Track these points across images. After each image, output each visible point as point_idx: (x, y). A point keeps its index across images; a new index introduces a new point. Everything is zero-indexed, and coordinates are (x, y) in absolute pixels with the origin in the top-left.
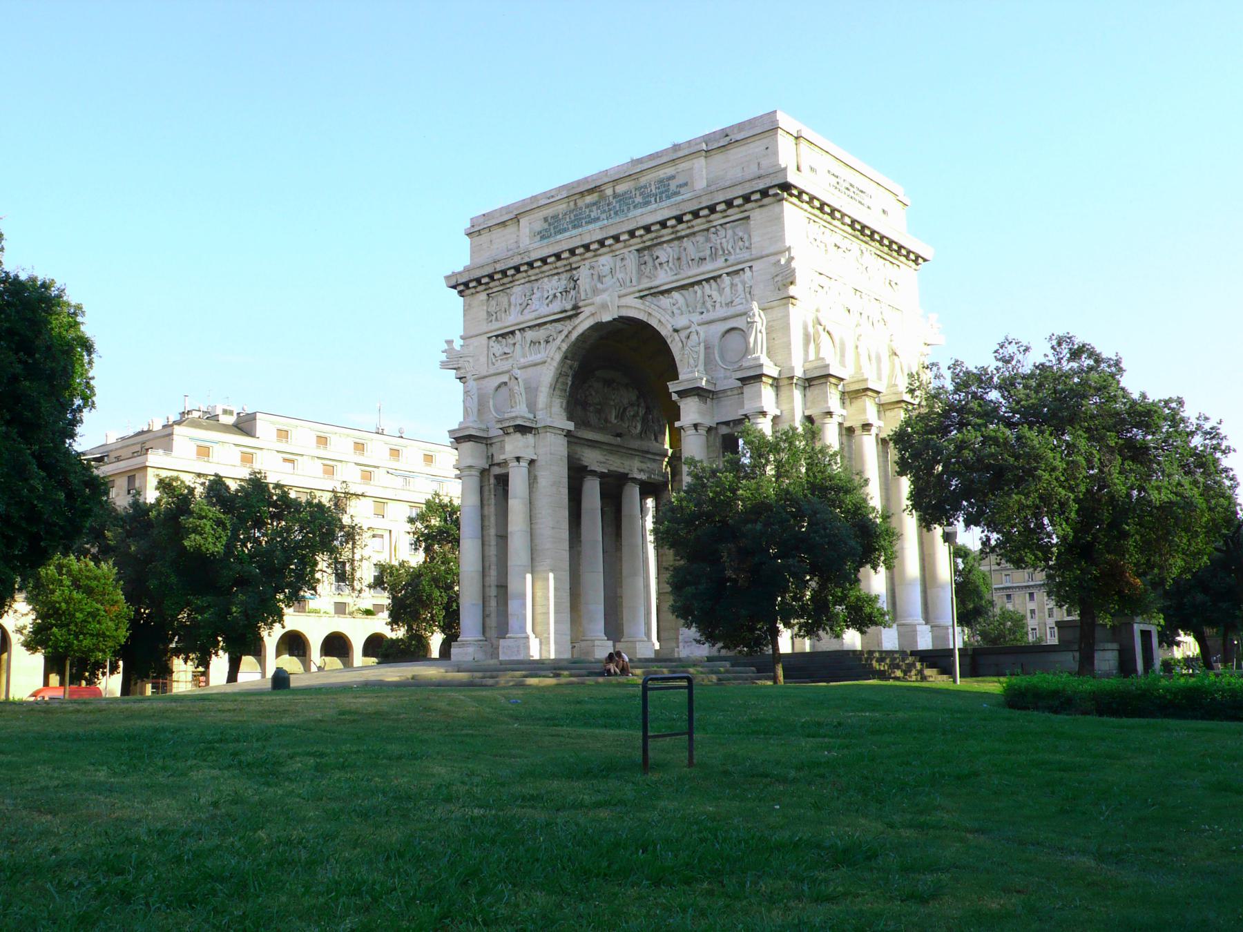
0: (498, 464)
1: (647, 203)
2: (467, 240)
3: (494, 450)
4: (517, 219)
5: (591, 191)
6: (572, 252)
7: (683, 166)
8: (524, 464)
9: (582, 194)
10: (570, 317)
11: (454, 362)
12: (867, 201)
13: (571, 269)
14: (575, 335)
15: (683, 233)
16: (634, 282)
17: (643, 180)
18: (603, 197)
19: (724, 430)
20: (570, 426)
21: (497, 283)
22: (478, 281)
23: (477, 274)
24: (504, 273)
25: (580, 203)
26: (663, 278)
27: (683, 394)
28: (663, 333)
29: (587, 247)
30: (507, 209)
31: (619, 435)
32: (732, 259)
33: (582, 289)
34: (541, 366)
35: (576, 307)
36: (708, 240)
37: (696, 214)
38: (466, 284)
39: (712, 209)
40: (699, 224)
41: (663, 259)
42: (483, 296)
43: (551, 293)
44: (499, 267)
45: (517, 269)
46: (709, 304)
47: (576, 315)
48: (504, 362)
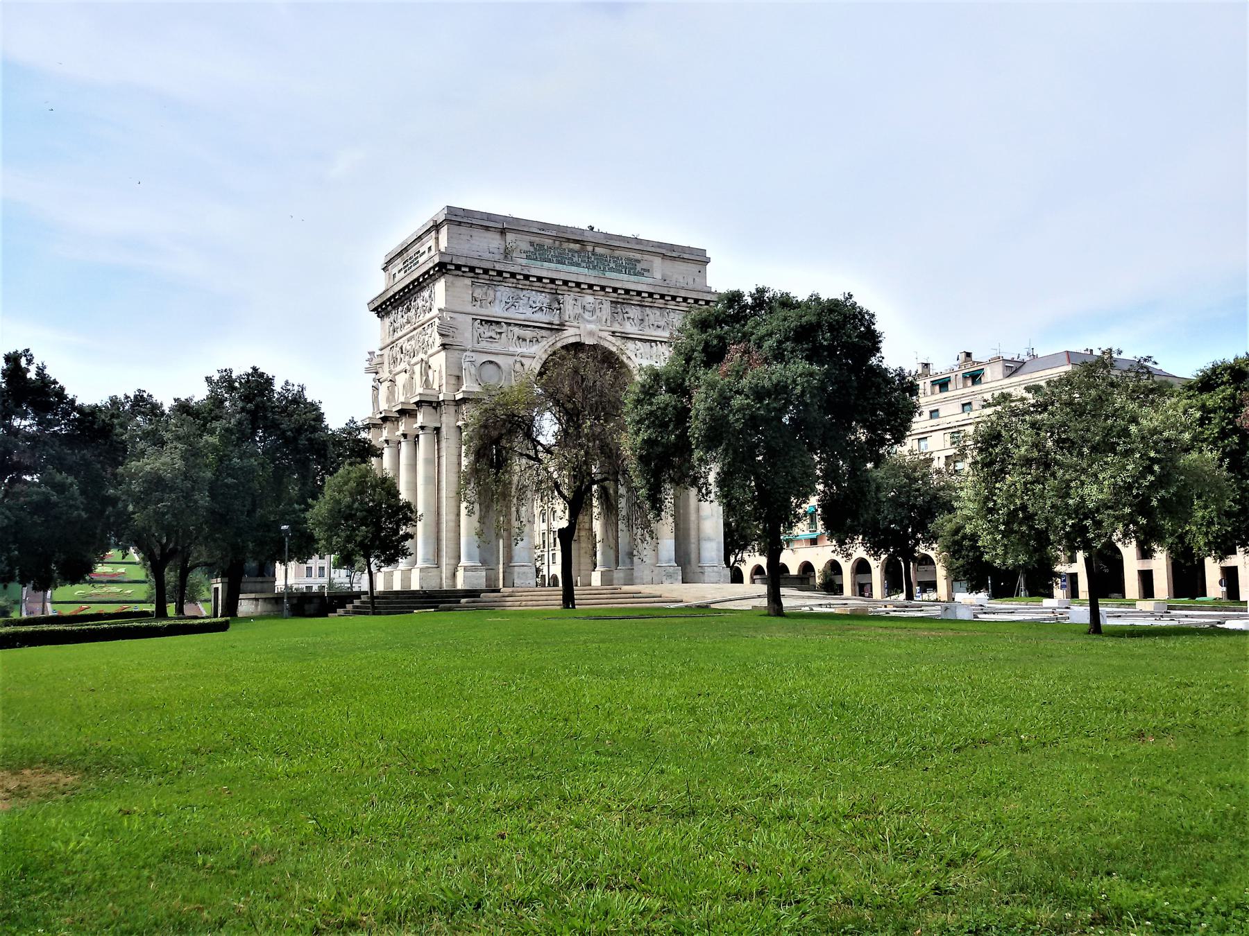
6: (566, 283)
7: (646, 257)
9: (569, 240)
10: (551, 329)
17: (617, 253)
18: (583, 249)
22: (472, 269)
23: (474, 263)
24: (500, 273)
25: (565, 245)
26: (630, 328)
29: (578, 284)
30: (489, 217)
35: (562, 324)
37: (662, 296)
38: (458, 267)
39: (674, 298)
43: (539, 305)
44: (499, 267)
45: (513, 275)
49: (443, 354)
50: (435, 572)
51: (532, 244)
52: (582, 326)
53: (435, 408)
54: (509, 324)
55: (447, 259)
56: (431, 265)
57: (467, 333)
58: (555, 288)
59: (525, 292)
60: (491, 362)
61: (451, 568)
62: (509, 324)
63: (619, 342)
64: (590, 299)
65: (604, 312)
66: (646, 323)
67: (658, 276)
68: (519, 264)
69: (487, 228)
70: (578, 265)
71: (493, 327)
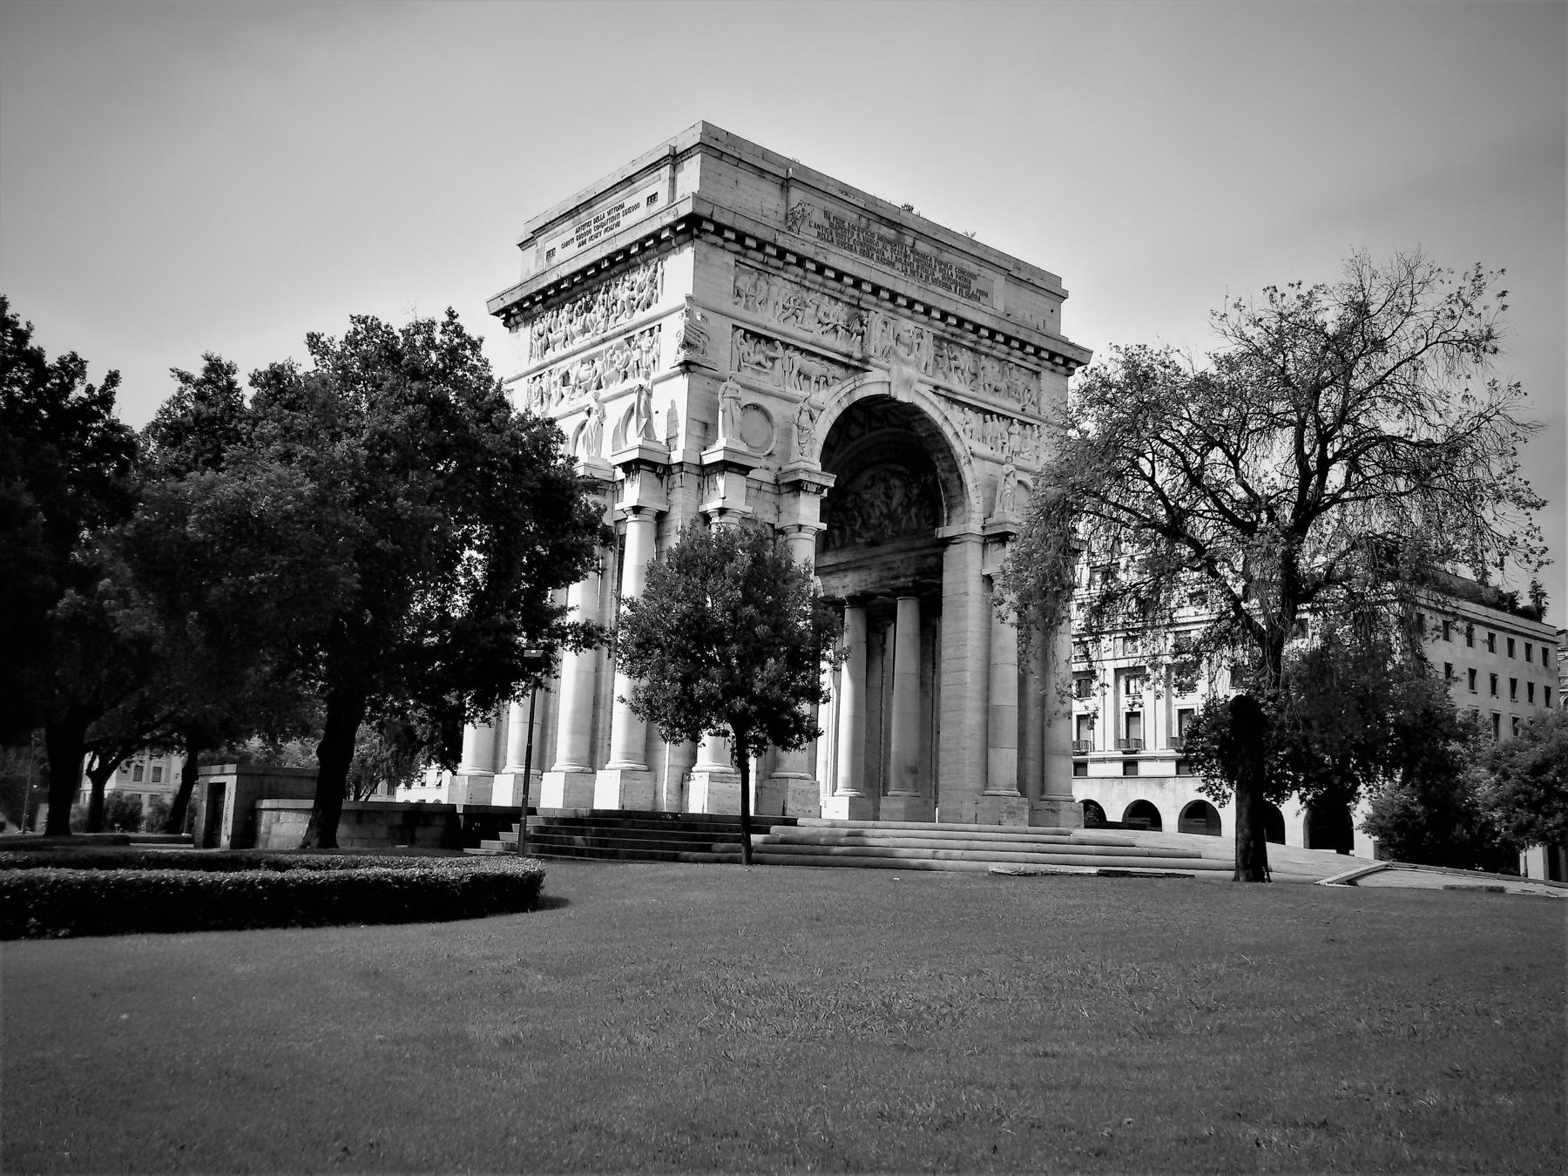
4: (785, 184)
5: (892, 224)
6: (876, 290)
7: (987, 273)
14: (858, 396)
15: (983, 349)
16: (930, 368)
17: (946, 257)
21: (760, 256)
22: (741, 237)
23: (746, 227)
24: (782, 253)
25: (875, 227)
28: (958, 449)
29: (894, 297)
33: (873, 343)
37: (1008, 340)
38: (720, 229)
39: (1023, 345)
48: (754, 375)
49: (683, 381)
50: (644, 780)
51: (827, 214)
52: (895, 368)
53: (660, 477)
54: (786, 346)
55: (705, 211)
56: (669, 219)
57: (724, 349)
59: (812, 295)
60: (757, 407)
61: (677, 772)
62: (786, 346)
63: (943, 405)
64: (910, 325)
65: (923, 351)
66: (980, 381)
67: (1000, 307)
69: (762, 173)
70: (891, 264)
71: (763, 346)
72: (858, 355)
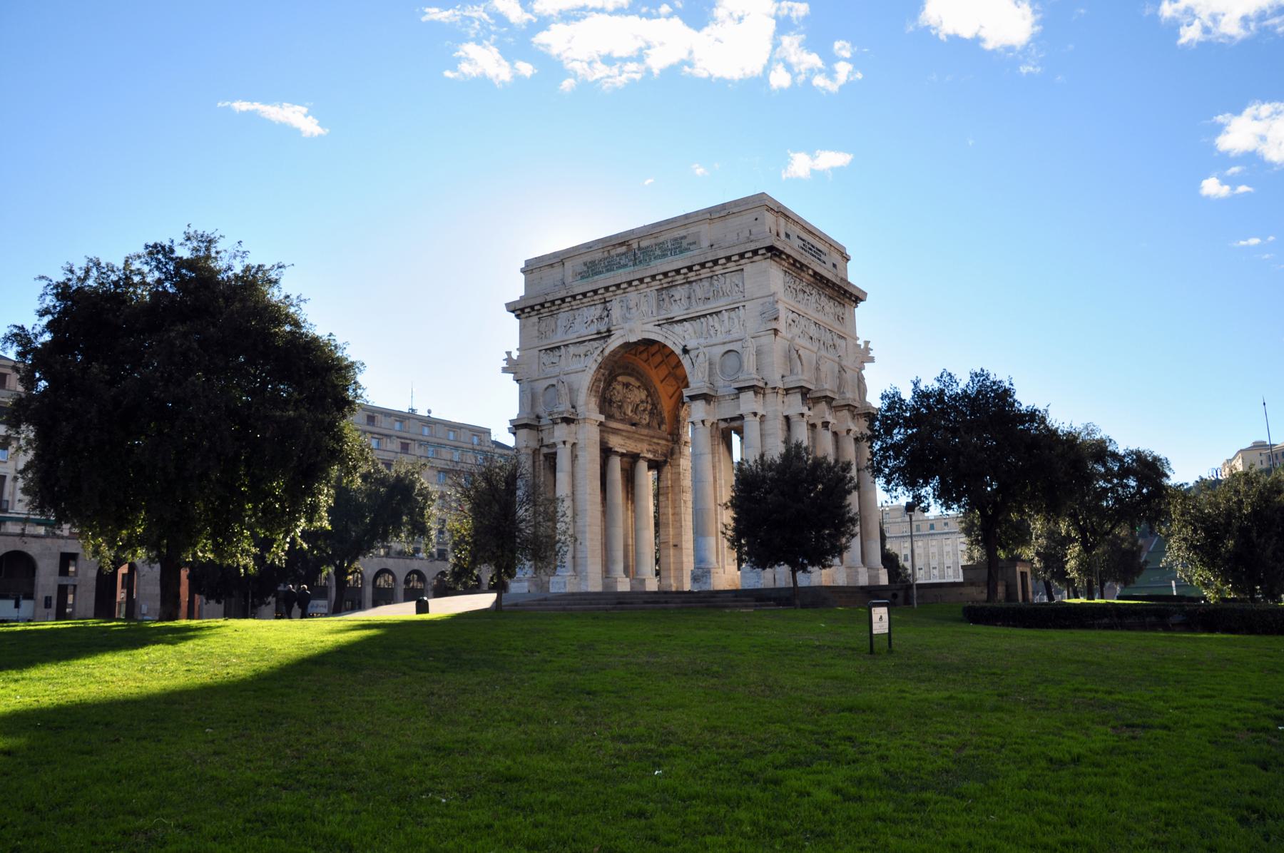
0: (547, 446)
1: (664, 256)
2: (523, 276)
3: (544, 435)
5: (622, 244)
6: (607, 289)
7: (693, 230)
8: (568, 446)
11: (512, 366)
12: (823, 257)
13: (605, 302)
14: (607, 352)
17: (661, 239)
19: (723, 425)
20: (602, 418)
22: (532, 308)
23: (531, 303)
24: (553, 302)
25: (613, 253)
26: (677, 311)
27: (693, 398)
29: (618, 286)
30: (555, 255)
31: (634, 425)
32: (729, 300)
34: (582, 372)
35: (609, 331)
36: (711, 284)
37: (703, 265)
38: (522, 310)
39: (715, 262)
40: (705, 273)
41: (677, 297)
42: (535, 319)
44: (550, 298)
45: (563, 300)
46: (712, 332)
47: (609, 336)
51: (585, 264)
58: (601, 296)
66: (693, 300)
67: (705, 244)
68: (579, 288)
70: (625, 266)
72: (603, 329)
